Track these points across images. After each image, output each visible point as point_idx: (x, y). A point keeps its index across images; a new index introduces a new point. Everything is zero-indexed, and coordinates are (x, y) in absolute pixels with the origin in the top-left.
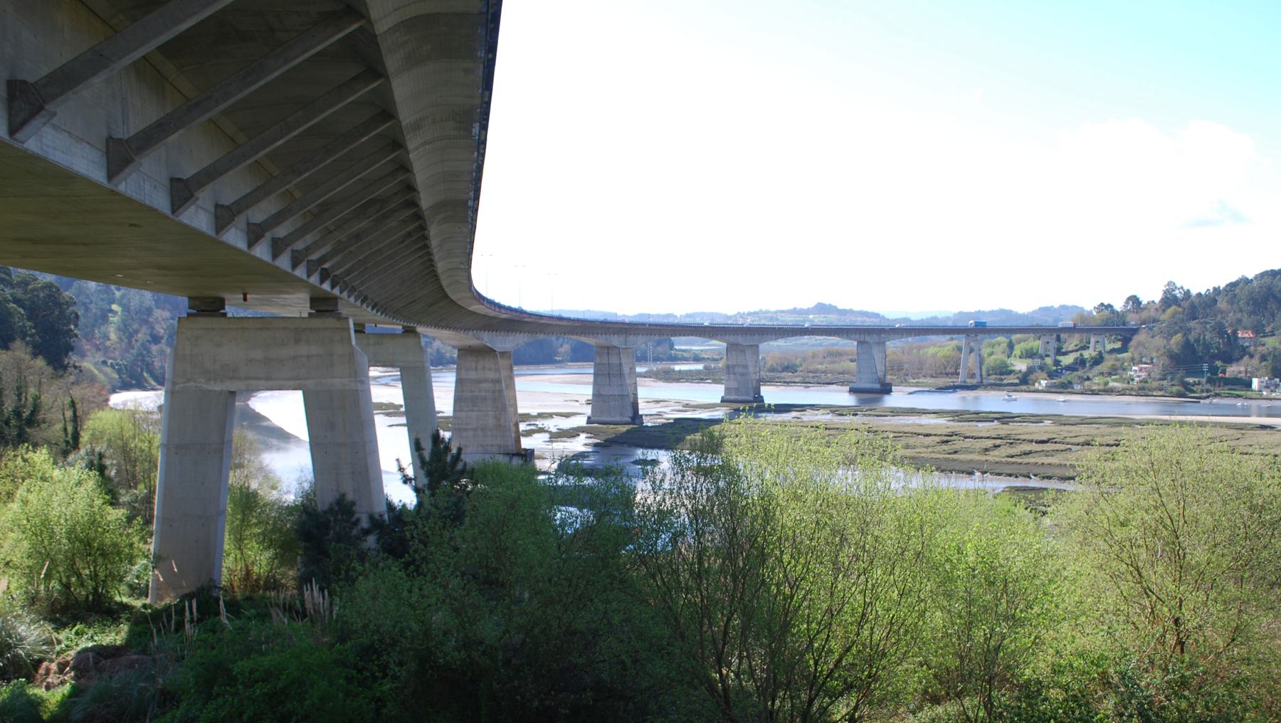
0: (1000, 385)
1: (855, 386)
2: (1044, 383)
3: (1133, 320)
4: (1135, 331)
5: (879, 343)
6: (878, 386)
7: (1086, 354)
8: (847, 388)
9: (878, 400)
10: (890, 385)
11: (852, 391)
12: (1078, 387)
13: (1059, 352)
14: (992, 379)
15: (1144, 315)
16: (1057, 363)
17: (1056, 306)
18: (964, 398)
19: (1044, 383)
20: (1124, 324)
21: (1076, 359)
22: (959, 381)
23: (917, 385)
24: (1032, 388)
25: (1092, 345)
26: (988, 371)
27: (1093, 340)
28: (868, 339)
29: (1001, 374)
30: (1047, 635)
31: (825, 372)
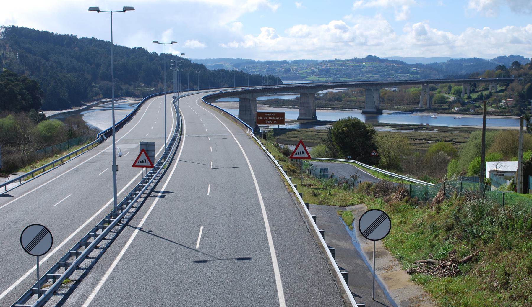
0: (439, 109)
1: (365, 110)
2: (456, 108)
3: (513, 74)
4: (512, 81)
5: (376, 90)
6: (375, 110)
7: (484, 93)
8: (361, 111)
9: (376, 118)
10: (382, 110)
11: (363, 113)
12: (472, 111)
13: (473, 92)
14: (437, 106)
15: (521, 71)
16: (469, 98)
17: (508, 56)
18: (421, 117)
19: (456, 108)
20: (509, 76)
21: (478, 96)
22: (419, 107)
23: (396, 109)
24: (451, 111)
25: (490, 88)
26: (435, 102)
27: (491, 85)
28: (370, 88)
29: (442, 103)
30: (520, 234)
31: (355, 101)
